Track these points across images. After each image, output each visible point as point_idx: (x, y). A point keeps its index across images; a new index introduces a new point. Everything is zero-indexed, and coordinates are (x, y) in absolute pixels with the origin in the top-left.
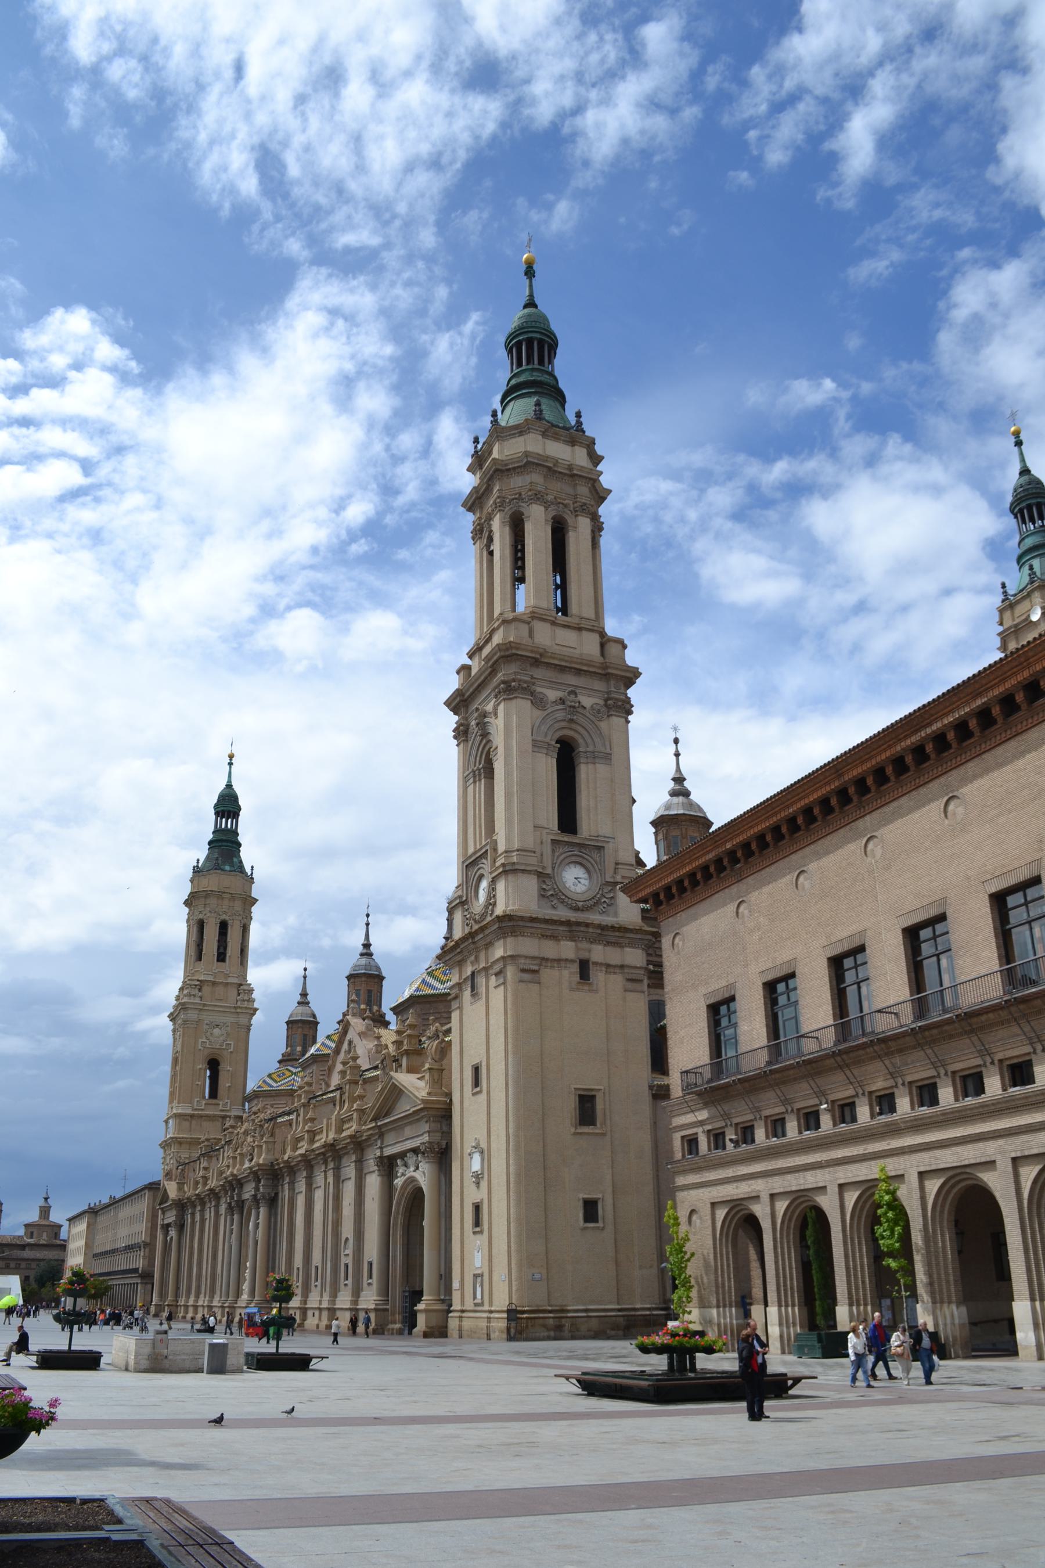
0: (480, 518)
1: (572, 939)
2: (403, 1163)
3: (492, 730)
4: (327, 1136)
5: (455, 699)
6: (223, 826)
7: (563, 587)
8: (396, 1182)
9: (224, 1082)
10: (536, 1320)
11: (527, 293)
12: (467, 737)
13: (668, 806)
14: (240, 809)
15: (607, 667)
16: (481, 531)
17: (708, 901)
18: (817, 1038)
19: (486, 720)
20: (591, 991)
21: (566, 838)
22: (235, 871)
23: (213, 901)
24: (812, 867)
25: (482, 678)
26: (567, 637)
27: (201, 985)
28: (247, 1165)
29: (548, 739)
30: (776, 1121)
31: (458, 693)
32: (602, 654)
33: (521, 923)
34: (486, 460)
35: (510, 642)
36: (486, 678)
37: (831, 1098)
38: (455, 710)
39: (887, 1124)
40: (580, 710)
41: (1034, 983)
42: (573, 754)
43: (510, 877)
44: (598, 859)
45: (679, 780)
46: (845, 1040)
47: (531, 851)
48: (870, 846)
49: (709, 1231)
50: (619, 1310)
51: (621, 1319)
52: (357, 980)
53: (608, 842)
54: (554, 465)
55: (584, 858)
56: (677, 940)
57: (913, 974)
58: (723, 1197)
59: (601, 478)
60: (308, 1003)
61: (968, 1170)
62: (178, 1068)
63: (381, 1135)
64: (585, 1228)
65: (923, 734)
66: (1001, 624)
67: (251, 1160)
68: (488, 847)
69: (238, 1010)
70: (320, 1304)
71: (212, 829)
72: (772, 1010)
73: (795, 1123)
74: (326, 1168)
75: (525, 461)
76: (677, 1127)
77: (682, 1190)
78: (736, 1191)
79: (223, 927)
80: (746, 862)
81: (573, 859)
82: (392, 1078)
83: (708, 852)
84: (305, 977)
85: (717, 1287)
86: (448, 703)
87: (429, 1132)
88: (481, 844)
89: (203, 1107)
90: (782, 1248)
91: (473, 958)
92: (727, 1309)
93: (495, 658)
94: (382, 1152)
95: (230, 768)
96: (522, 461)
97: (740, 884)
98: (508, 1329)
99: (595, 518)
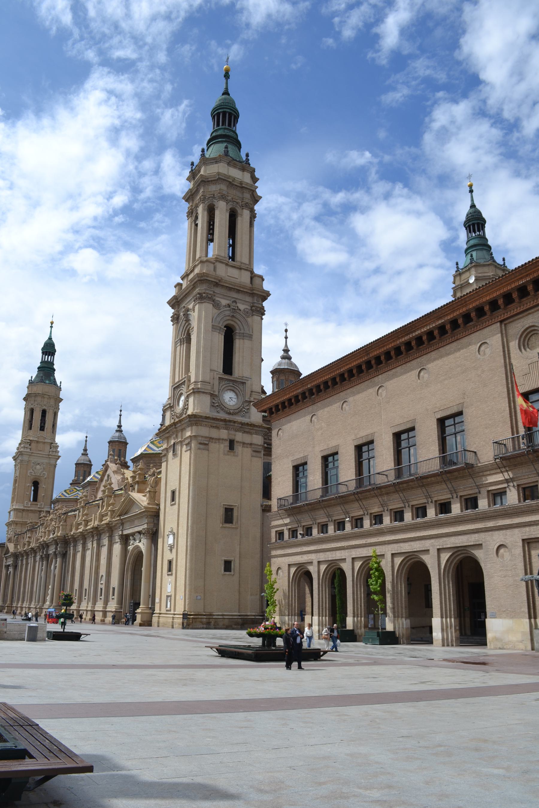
0: (192, 206)
1: (226, 429)
2: (133, 538)
3: (191, 318)
4: (94, 523)
5: (173, 300)
6: (46, 360)
7: (233, 246)
8: (129, 547)
9: (41, 493)
10: (197, 619)
11: (225, 87)
12: (178, 321)
13: (280, 364)
14: (55, 351)
15: (253, 290)
16: (192, 213)
17: (297, 413)
18: (347, 485)
19: (189, 313)
20: (234, 456)
21: (226, 377)
22: (51, 384)
23: (39, 399)
24: (350, 399)
25: (188, 291)
26: (233, 273)
27: (31, 442)
28: (51, 536)
29: (220, 325)
30: (323, 525)
31: (175, 297)
32: (251, 283)
33: (201, 419)
34: (197, 175)
35: (204, 273)
37: (352, 515)
38: (173, 307)
39: (378, 530)
40: (238, 311)
41: (455, 464)
42: (233, 334)
43: (196, 395)
44: (242, 389)
45: (286, 351)
46: (360, 487)
47: (207, 383)
48: (380, 391)
49: (287, 578)
50: (239, 616)
51: (240, 620)
52: (114, 443)
53: (248, 380)
54: (233, 181)
55: (235, 388)
56: (280, 432)
57: (396, 456)
58: (294, 562)
59: (257, 190)
60: (87, 454)
61: (416, 554)
62: (17, 485)
63: (122, 524)
64: (224, 575)
65: (411, 336)
66: (454, 283)
67: (54, 534)
68: (186, 379)
69: (50, 457)
70: (87, 608)
71: (40, 361)
72: (325, 470)
73: (333, 527)
74: (93, 539)
75: (218, 177)
76: (274, 526)
77: (275, 558)
78: (301, 559)
79: (44, 413)
80: (317, 395)
81: (230, 388)
82: (129, 495)
83: (299, 389)
84: (86, 441)
85: (289, 606)
86: (169, 303)
87: (147, 523)
88: (182, 377)
89: (29, 506)
90: (322, 588)
91: (175, 436)
92: (293, 617)
93: (195, 280)
94: (122, 532)
95: (51, 329)
96: (216, 177)
97: (314, 406)
98: (183, 624)
99: (252, 211)
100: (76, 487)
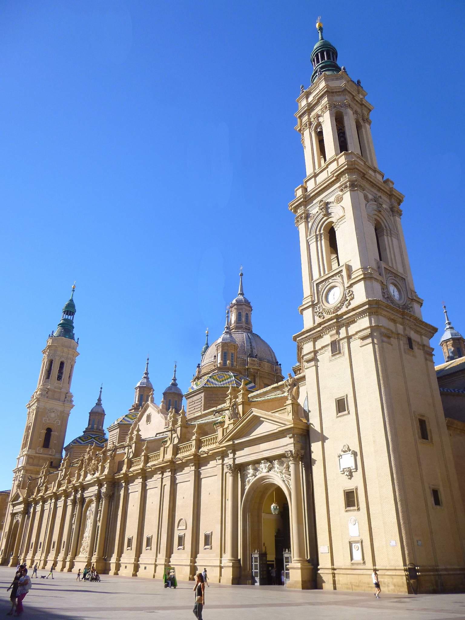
4: (164, 457)
9: (53, 440)
14: (75, 312)
16: (310, 124)
19: (329, 206)
36: (328, 185)
79: (62, 364)
84: (101, 392)
89: (41, 452)
91: (334, 332)
100: (90, 435)
